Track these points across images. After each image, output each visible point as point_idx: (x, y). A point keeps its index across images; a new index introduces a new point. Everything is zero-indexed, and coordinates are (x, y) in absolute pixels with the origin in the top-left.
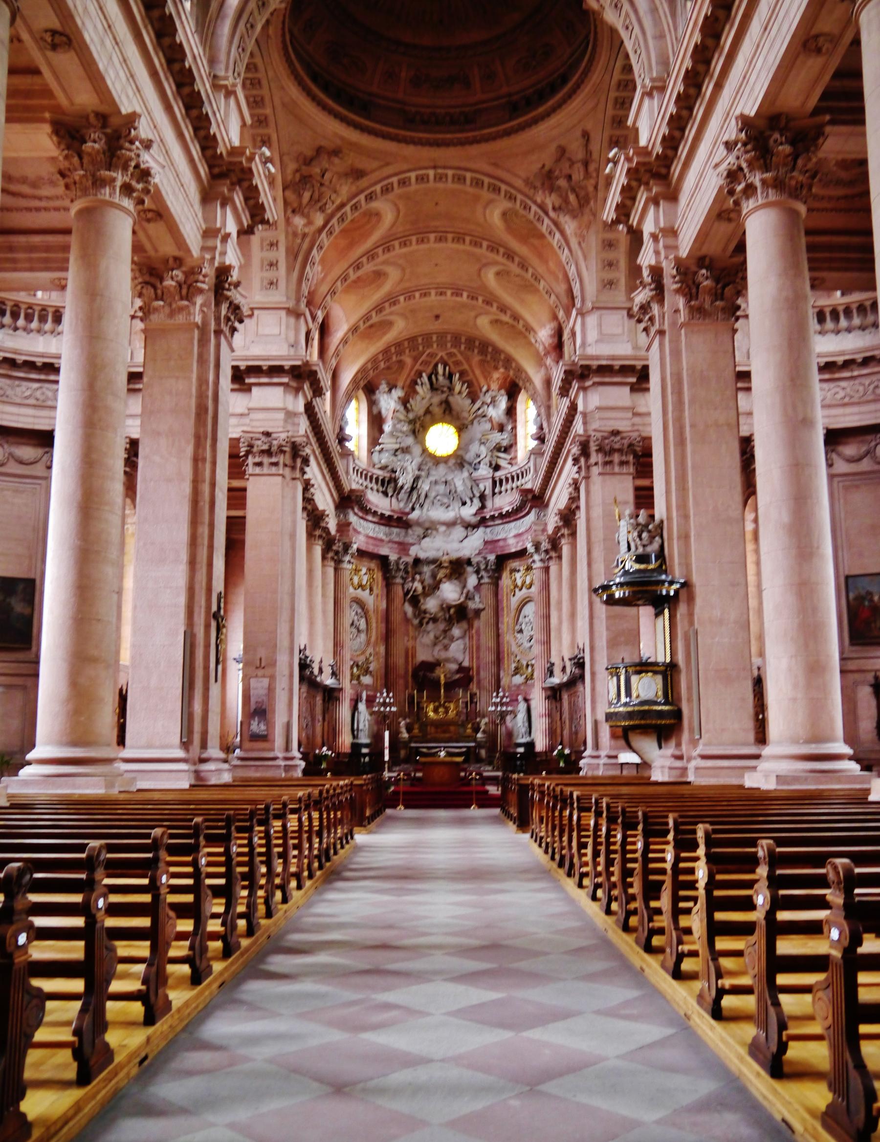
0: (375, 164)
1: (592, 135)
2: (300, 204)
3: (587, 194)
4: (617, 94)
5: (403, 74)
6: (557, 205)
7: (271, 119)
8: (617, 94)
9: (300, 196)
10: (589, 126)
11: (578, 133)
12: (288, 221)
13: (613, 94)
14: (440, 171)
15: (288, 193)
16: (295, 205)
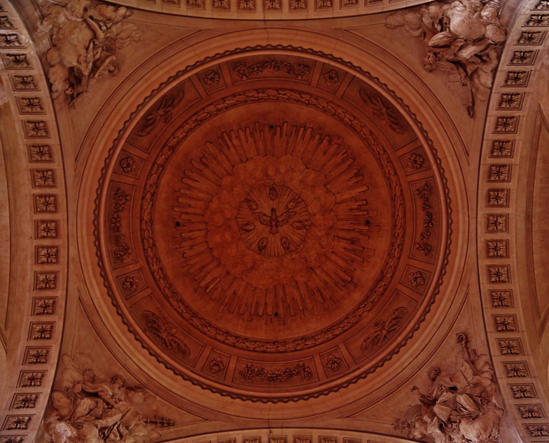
0: (189, 417)
1: (471, 331)
2: (73, 413)
3: (484, 390)
4: (489, 262)
5: (232, 366)
6: (444, 419)
7: (61, 303)
8: (489, 262)
9: (75, 404)
10: (462, 325)
11: (452, 340)
12: (47, 427)
13: (484, 262)
14: (276, 432)
15: (56, 395)
16: (65, 412)
